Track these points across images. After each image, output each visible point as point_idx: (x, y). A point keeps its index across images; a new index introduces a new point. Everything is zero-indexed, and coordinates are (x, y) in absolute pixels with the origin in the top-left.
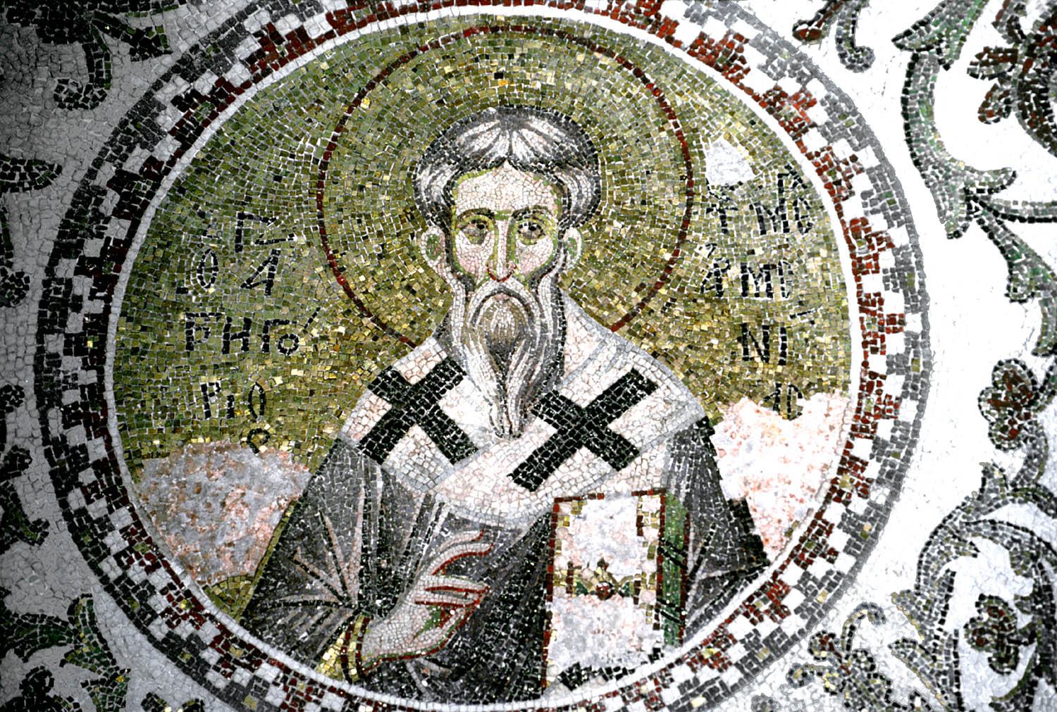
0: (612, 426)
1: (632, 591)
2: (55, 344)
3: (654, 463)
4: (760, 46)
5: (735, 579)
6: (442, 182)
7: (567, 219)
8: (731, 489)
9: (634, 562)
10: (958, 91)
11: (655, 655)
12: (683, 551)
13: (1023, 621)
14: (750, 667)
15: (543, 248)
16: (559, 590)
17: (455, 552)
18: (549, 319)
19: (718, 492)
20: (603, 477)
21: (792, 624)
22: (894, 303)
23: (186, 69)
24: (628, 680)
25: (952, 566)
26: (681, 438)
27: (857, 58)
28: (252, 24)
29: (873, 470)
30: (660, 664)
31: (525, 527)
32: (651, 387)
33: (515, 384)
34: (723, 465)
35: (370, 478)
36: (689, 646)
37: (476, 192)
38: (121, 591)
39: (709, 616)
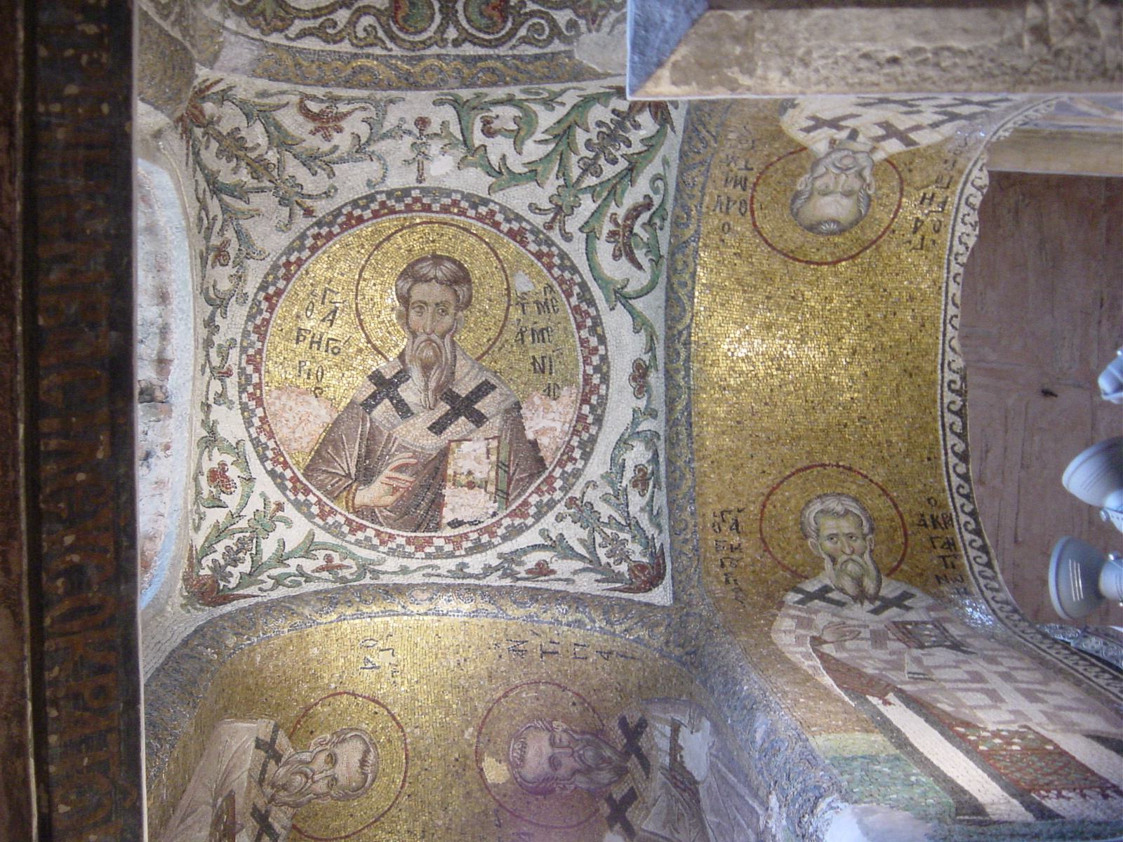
0: (476, 407)
1: (484, 485)
2: (250, 328)
3: (494, 424)
4: (532, 232)
5: (532, 477)
6: (407, 286)
7: (458, 308)
8: (530, 435)
9: (484, 471)
10: (604, 250)
11: (494, 514)
12: (508, 466)
13: (650, 468)
14: (539, 516)
15: (448, 320)
16: (449, 484)
17: (401, 462)
18: (449, 356)
19: (524, 436)
20: (471, 432)
21: (558, 495)
22: (594, 341)
23: (319, 224)
24: (481, 526)
25: (625, 456)
26: (507, 411)
27: (568, 237)
28: (344, 211)
29: (590, 419)
30: (496, 518)
31: (434, 453)
32: (494, 387)
33: (432, 385)
34: (527, 424)
35: (364, 420)
36: (510, 509)
37: (419, 292)
38: (256, 443)
39: (519, 495)
